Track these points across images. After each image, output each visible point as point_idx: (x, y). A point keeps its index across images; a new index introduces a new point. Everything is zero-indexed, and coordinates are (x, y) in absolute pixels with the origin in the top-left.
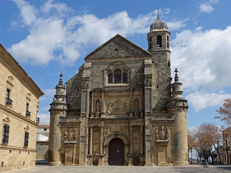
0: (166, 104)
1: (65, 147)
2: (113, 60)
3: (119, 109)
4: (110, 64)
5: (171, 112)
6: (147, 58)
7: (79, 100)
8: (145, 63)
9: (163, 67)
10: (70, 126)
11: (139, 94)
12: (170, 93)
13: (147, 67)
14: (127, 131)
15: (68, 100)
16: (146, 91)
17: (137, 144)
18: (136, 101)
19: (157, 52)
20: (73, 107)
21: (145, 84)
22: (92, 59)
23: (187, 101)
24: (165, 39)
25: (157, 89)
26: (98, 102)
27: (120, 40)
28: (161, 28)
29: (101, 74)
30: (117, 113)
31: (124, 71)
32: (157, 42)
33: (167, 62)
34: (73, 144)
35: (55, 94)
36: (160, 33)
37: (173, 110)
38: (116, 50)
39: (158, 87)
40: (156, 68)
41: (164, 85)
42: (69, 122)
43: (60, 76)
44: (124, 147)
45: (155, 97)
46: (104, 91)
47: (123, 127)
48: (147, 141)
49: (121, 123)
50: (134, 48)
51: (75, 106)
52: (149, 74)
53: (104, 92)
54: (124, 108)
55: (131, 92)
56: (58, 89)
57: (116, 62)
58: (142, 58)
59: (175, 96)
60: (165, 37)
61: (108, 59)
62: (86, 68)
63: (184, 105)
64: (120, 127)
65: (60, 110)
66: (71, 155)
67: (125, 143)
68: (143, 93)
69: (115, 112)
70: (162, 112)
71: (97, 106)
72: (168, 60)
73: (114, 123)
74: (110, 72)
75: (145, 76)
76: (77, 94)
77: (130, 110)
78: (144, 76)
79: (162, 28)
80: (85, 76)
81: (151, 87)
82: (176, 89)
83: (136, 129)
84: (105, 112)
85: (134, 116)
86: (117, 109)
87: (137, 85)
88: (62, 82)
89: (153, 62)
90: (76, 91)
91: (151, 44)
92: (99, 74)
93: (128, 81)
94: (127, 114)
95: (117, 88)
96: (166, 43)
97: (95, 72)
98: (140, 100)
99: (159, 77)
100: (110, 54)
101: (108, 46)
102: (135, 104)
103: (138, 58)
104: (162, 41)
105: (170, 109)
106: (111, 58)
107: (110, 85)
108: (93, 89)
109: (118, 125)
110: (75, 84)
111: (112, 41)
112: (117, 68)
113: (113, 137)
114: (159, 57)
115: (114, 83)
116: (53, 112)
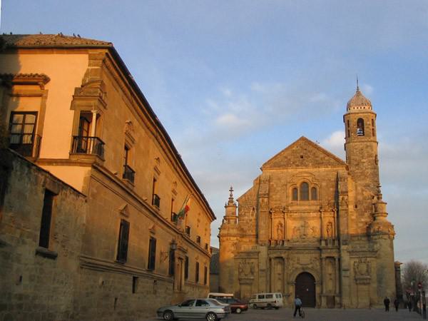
1: (240, 284)
14: (318, 264)
16: (341, 213)
27: (305, 144)
47: (313, 259)
48: (345, 276)
52: (344, 190)
60: (368, 121)
76: (252, 215)
85: (327, 244)
89: (349, 174)
94: (318, 241)
97: (275, 186)
99: (357, 194)
100: (293, 163)
101: (289, 152)
103: (330, 168)
104: (365, 126)
113: (302, 271)
116: (225, 238)
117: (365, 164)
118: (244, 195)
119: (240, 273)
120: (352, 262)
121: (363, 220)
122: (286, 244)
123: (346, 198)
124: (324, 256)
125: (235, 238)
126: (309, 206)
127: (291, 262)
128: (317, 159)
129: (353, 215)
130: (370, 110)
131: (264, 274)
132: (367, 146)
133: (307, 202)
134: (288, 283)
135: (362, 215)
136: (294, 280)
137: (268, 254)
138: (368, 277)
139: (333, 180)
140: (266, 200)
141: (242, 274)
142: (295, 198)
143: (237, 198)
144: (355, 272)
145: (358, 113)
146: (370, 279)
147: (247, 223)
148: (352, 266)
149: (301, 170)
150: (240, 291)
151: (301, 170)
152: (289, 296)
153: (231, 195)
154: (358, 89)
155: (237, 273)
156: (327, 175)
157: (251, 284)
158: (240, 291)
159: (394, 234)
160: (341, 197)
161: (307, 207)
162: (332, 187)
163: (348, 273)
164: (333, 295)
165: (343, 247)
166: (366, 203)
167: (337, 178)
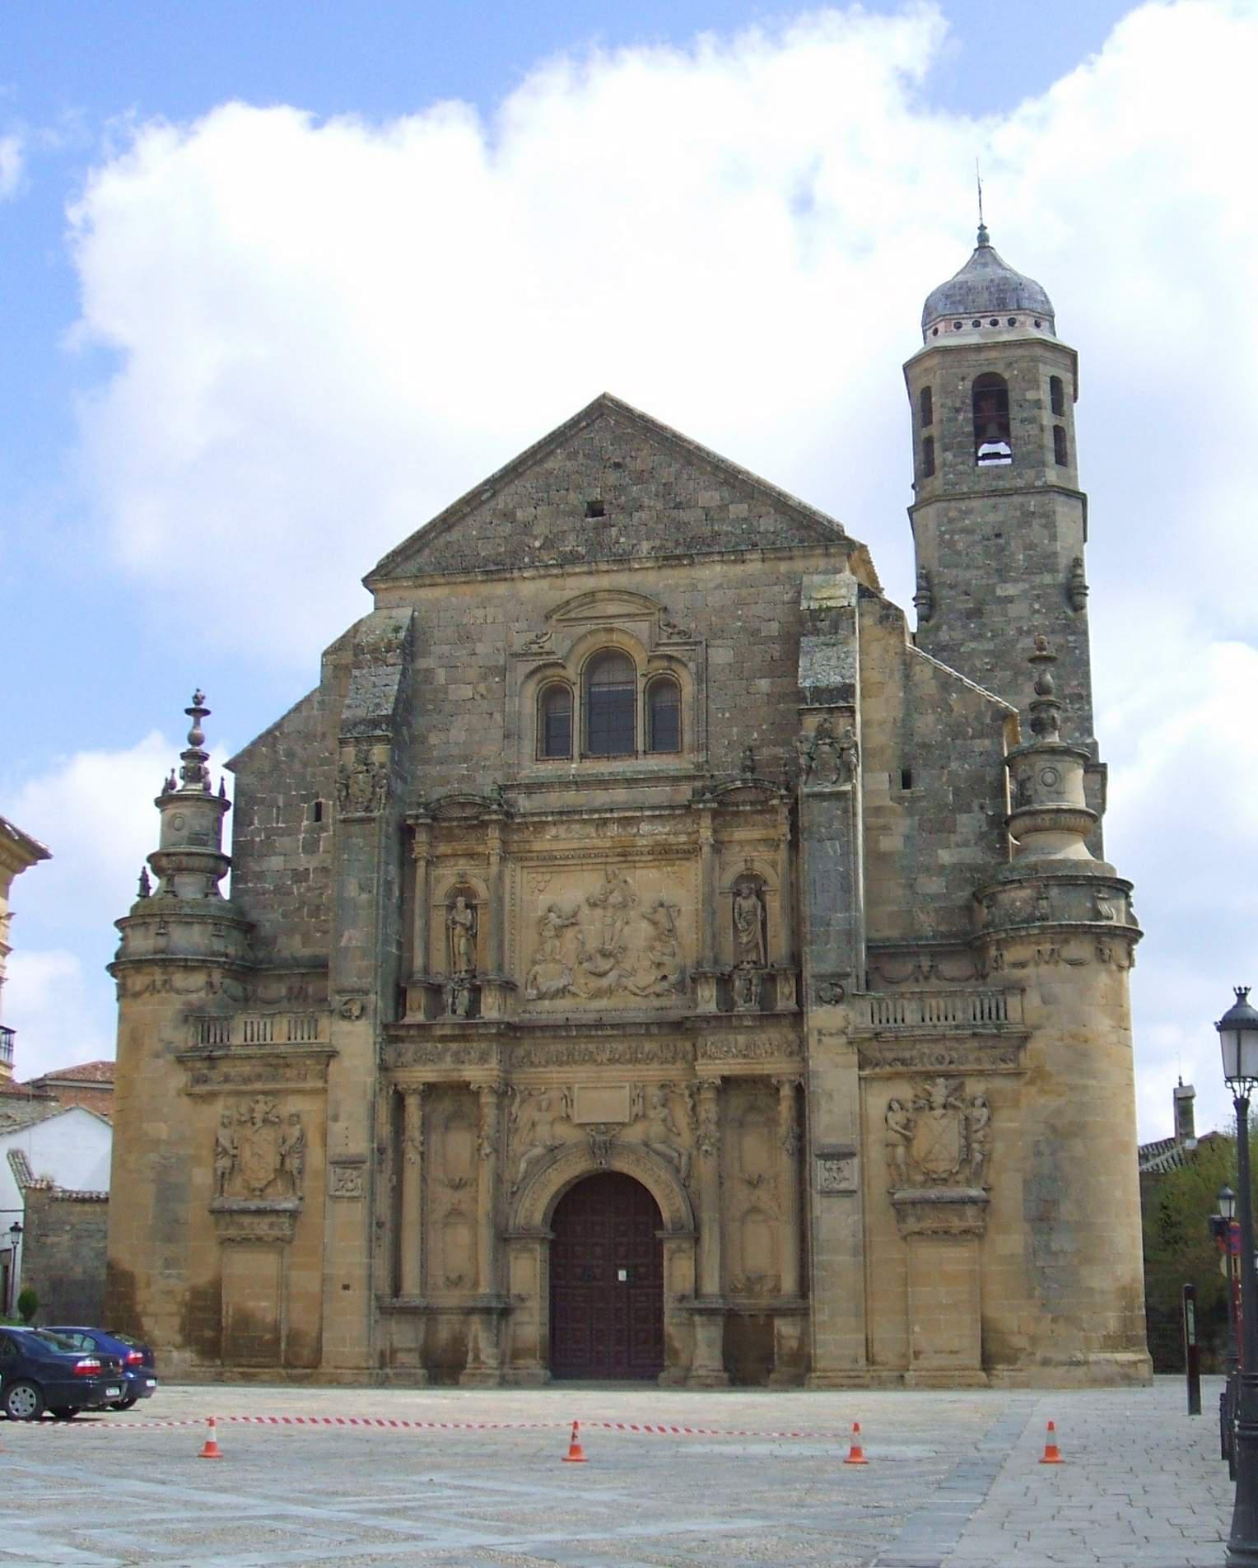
0: (968, 910)
2: (571, 582)
3: (624, 949)
4: (548, 617)
5: (1006, 971)
6: (822, 563)
7: (326, 886)
8: (804, 605)
9: (1026, 613)
10: (258, 1086)
11: (772, 833)
12: (1000, 823)
13: (817, 632)
14: (682, 1118)
15: (246, 891)
16: (812, 813)
17: (759, 1217)
18: (744, 886)
19: (976, 504)
20: (282, 941)
21: (803, 761)
22: (420, 579)
23: (1130, 886)
24: (1038, 404)
25: (900, 800)
26: (461, 902)
27: (617, 440)
28: (1003, 321)
29: (485, 693)
30: (604, 983)
31: (657, 664)
32: (970, 428)
33: (1061, 577)
34: (273, 1219)
35: (155, 847)
36: (993, 354)
37: (1013, 954)
38: (595, 510)
39: (907, 782)
40: (893, 641)
41: (954, 765)
42: (249, 1057)
43: (188, 712)
44: (660, 1243)
45: (891, 854)
46: (509, 820)
47: (654, 1093)
48: (828, 1193)
49: (637, 1061)
50: (726, 494)
51: (297, 939)
52: (836, 680)
53: (504, 827)
54: (657, 944)
55: (706, 821)
56: (172, 810)
57: (591, 596)
58: (783, 567)
59: (1042, 850)
60: (1035, 384)
61: (533, 578)
62: (375, 650)
63: (1098, 915)
64: (627, 1091)
65: (186, 967)
66: (264, 1304)
67: (666, 1215)
68: (791, 831)
69: (593, 977)
70: (948, 968)
71: (459, 930)
72: (1064, 562)
73: (584, 1061)
74: (549, 672)
75: (803, 700)
76: (311, 847)
77: (699, 964)
78: (799, 696)
79: (1012, 322)
80: (361, 713)
81: (845, 781)
82: (1036, 791)
83: (752, 1108)
84: (519, 979)
85: (726, 1001)
86: (606, 955)
87: (753, 770)
88: (205, 757)
90: (305, 823)
91: (929, 442)
92: (468, 691)
93: (687, 738)
94: (680, 986)
95: (601, 797)
96: (1042, 429)
97: (441, 676)
98: (775, 880)
99: (912, 706)
100: (548, 544)
101: (525, 485)
102: (738, 913)
103: (758, 565)
104: (1015, 413)
105: (993, 952)
106: (555, 571)
107: (549, 769)
108: (426, 806)
109: (613, 1072)
110: (297, 766)
111: (560, 445)
112: (602, 640)
113: (576, 1166)
114: (998, 536)
115: (583, 757)
116: (138, 982)
117: (1014, 610)
118: (269, 738)
119: (222, 1180)
120: (877, 1101)
121: (945, 857)
122: (491, 1008)
123: (842, 724)
124: (712, 1069)
125: (199, 979)
126: (630, 782)
127: (524, 1113)
128: (684, 515)
129: (885, 829)
130: (1036, 334)
131: (357, 1181)
132: (1028, 516)
133: (622, 766)
134: (504, 1239)
135: (940, 827)
136: (538, 1218)
137: (383, 1068)
138: (974, 1192)
139: (774, 627)
140: (379, 753)
141: (238, 1183)
142: (553, 743)
143: (226, 760)
144: (891, 1164)
145: (978, 348)
146: (983, 1205)
147: (280, 890)
148: (876, 1136)
149: (590, 583)
150: (217, 1285)
151: (590, 583)
152: (505, 1312)
153: (196, 740)
154: (983, 238)
155: (202, 1177)
156: (740, 603)
157: (280, 1244)
158: (217, 1285)
159: (1132, 935)
160: (811, 723)
161: (620, 795)
162: (770, 674)
163: (851, 1167)
164: (765, 1302)
165: (820, 1016)
166: (962, 757)
167: (801, 622)
